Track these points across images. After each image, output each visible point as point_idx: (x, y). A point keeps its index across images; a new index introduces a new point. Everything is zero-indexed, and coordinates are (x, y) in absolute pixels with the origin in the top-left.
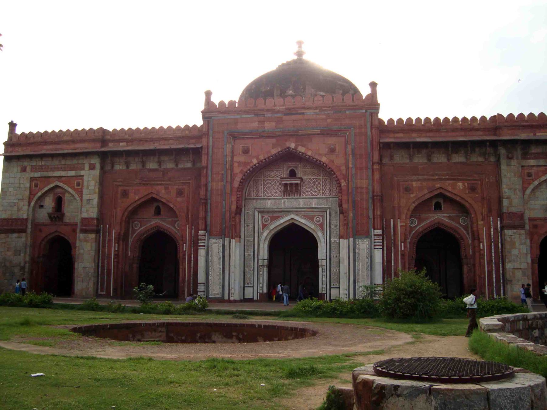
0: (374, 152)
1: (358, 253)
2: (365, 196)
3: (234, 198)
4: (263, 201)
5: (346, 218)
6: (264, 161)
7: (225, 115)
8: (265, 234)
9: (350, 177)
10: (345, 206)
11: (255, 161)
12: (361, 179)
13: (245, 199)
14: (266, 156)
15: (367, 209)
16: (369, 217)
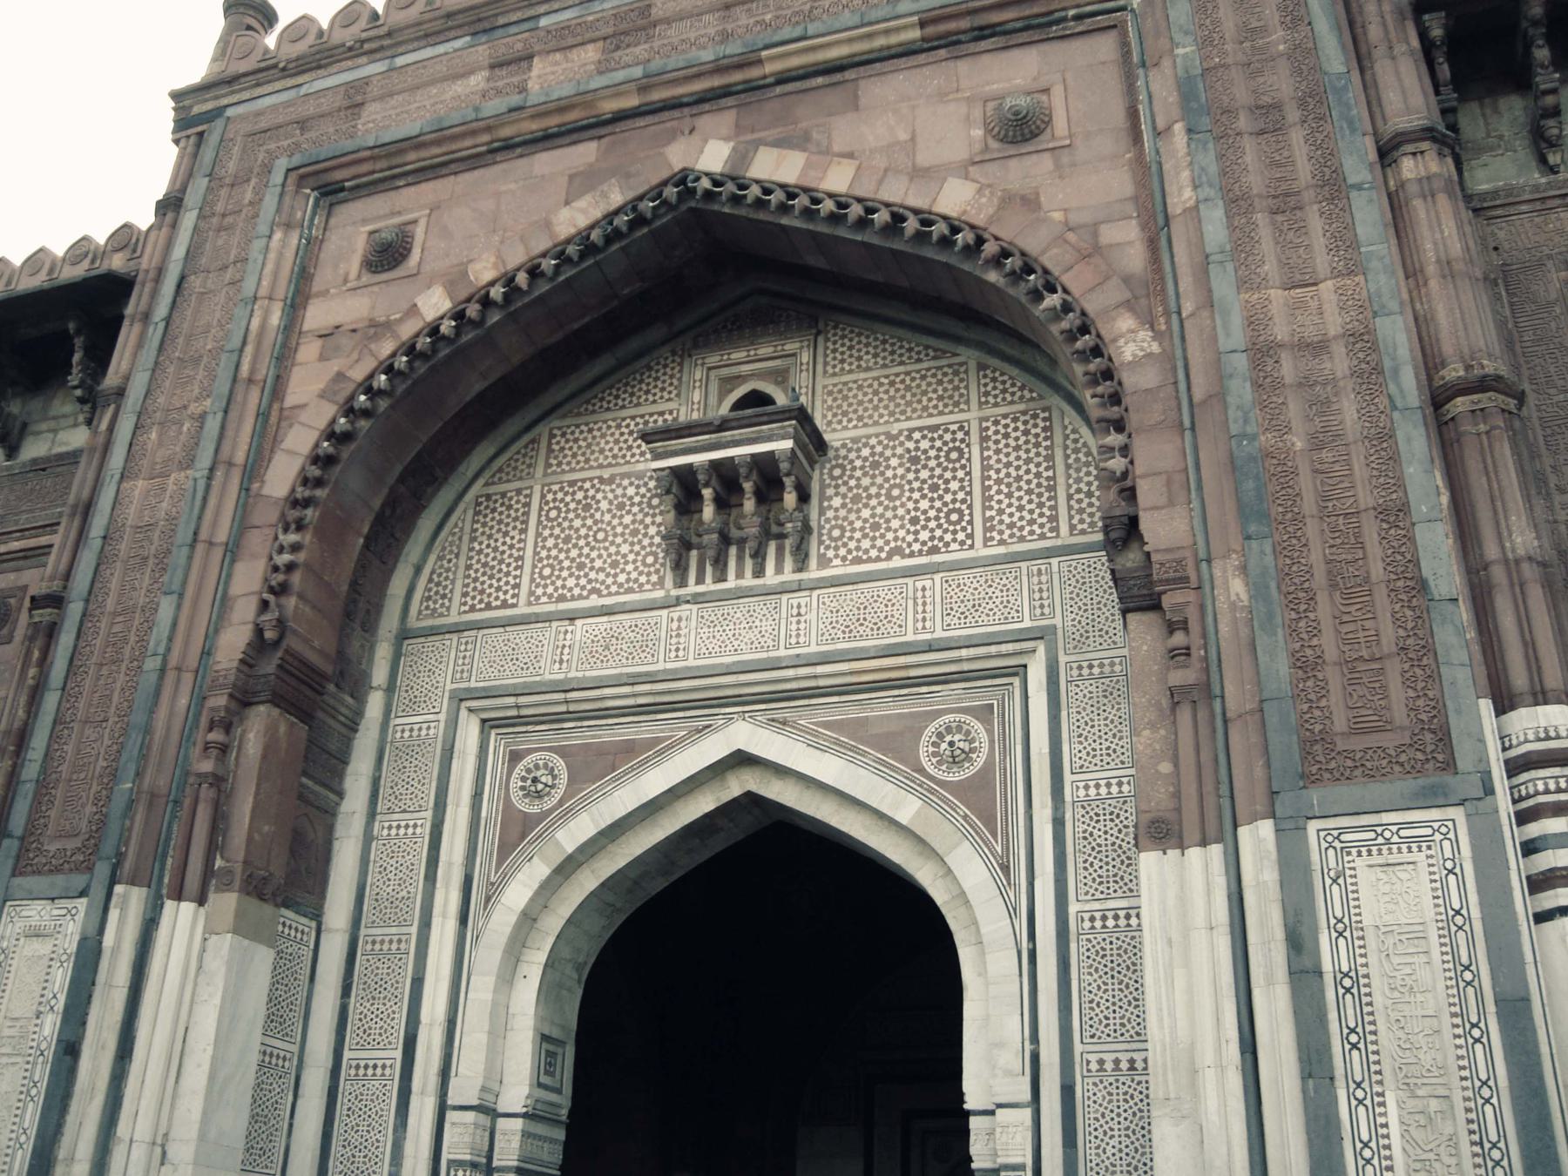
0: (1383, 70)
1: (1353, 983)
2: (1349, 411)
3: (249, 578)
4: (519, 635)
5: (1184, 635)
6: (497, 293)
7: (300, 80)
8: (518, 893)
9: (1186, 283)
10: (1163, 529)
11: (435, 304)
12: (1299, 280)
13: (404, 635)
14: (516, 257)
15: (1396, 513)
16: (1422, 586)
